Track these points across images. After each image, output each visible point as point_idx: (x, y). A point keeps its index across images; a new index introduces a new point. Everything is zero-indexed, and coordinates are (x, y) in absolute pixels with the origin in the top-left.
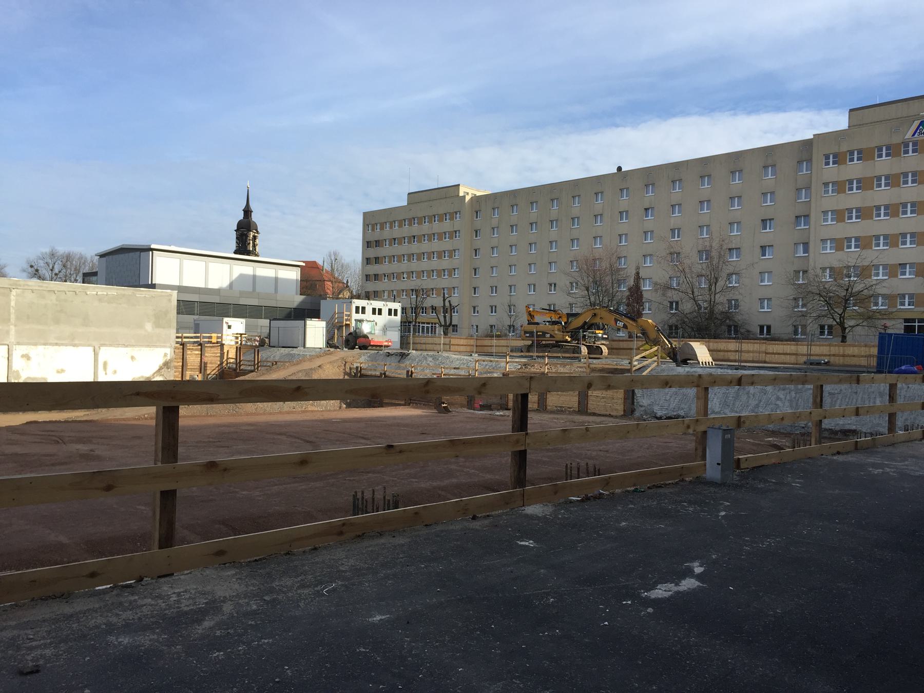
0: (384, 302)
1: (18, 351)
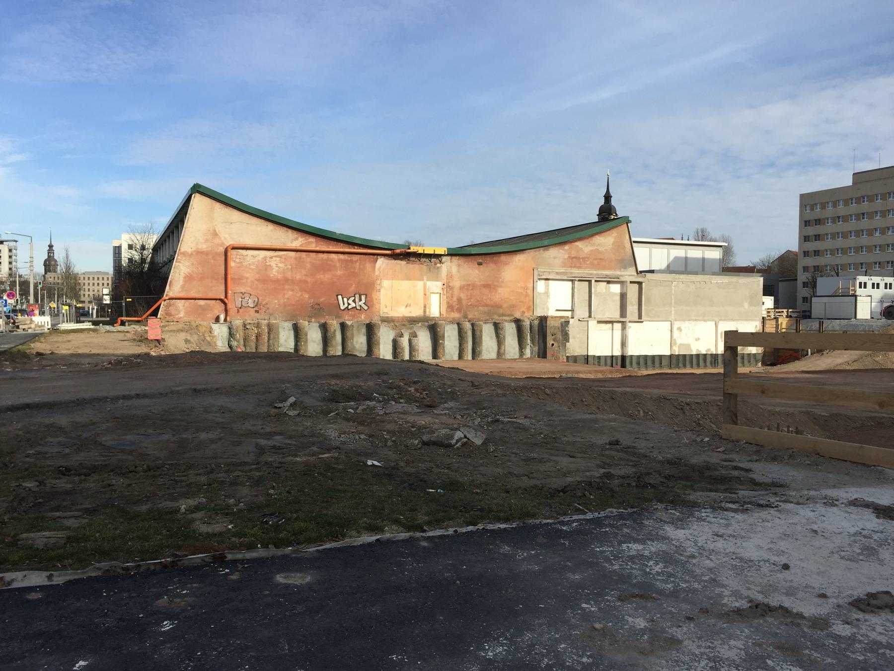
0: (881, 278)
1: (677, 325)
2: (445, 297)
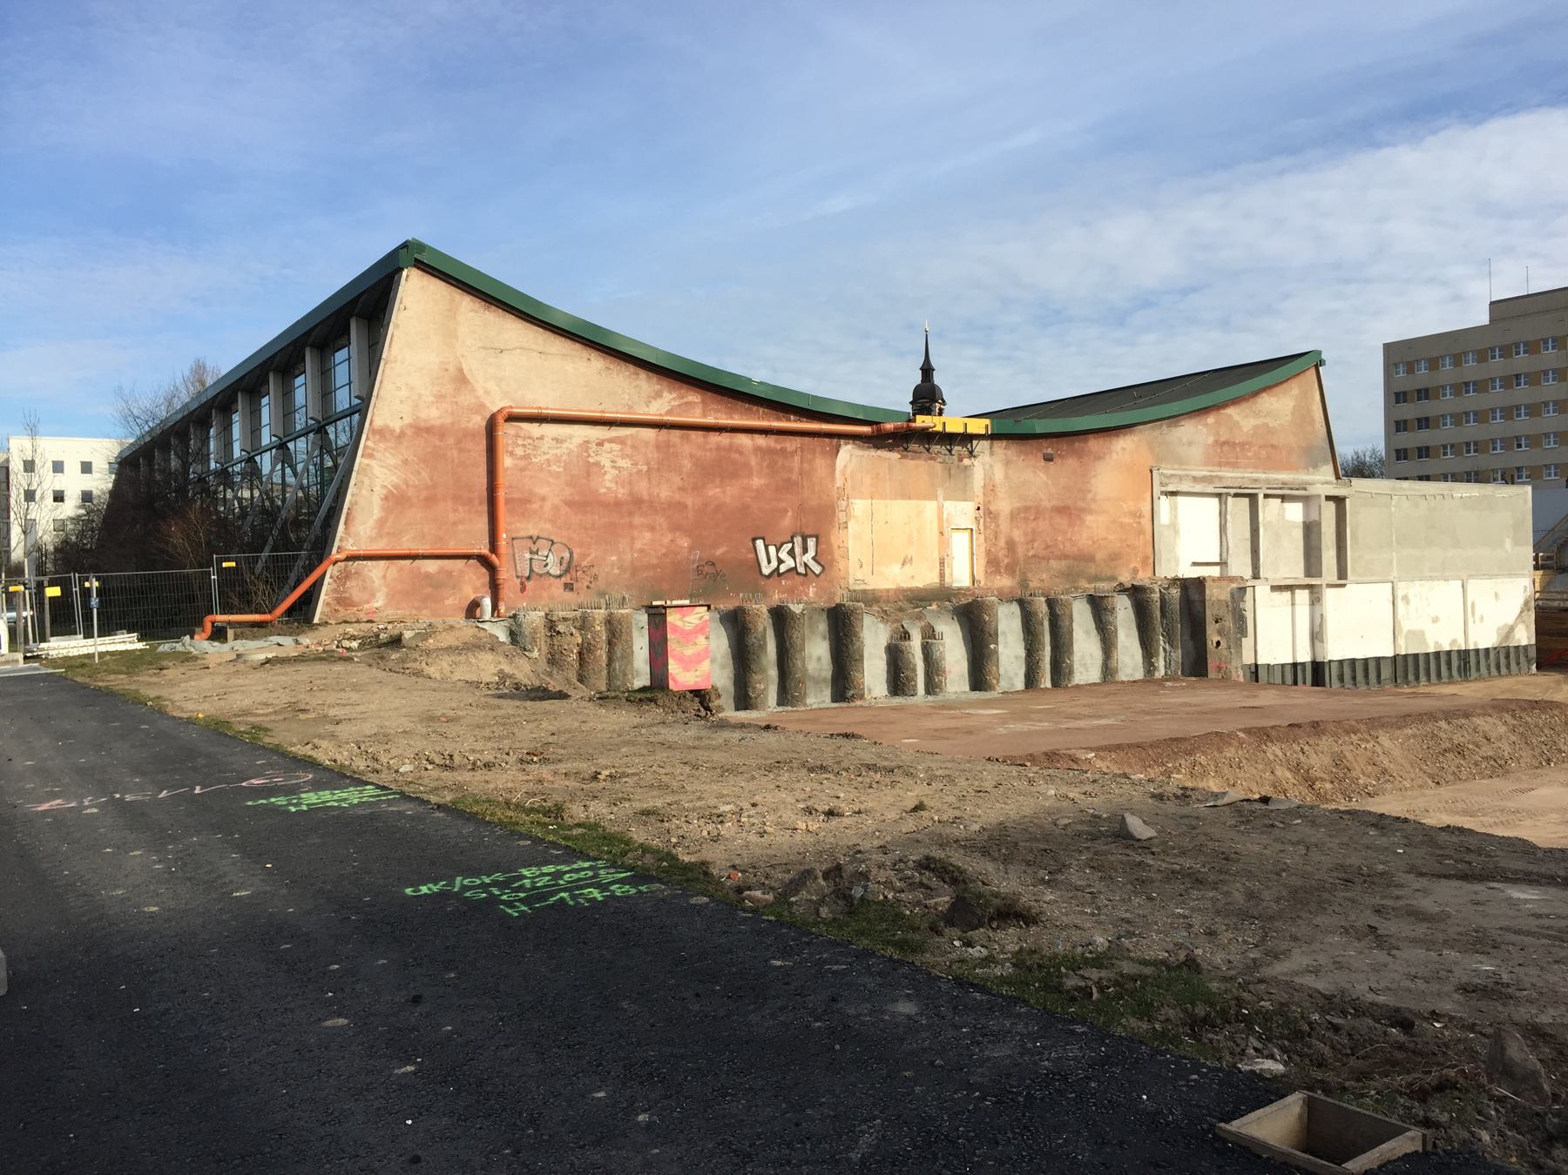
2: (982, 537)
